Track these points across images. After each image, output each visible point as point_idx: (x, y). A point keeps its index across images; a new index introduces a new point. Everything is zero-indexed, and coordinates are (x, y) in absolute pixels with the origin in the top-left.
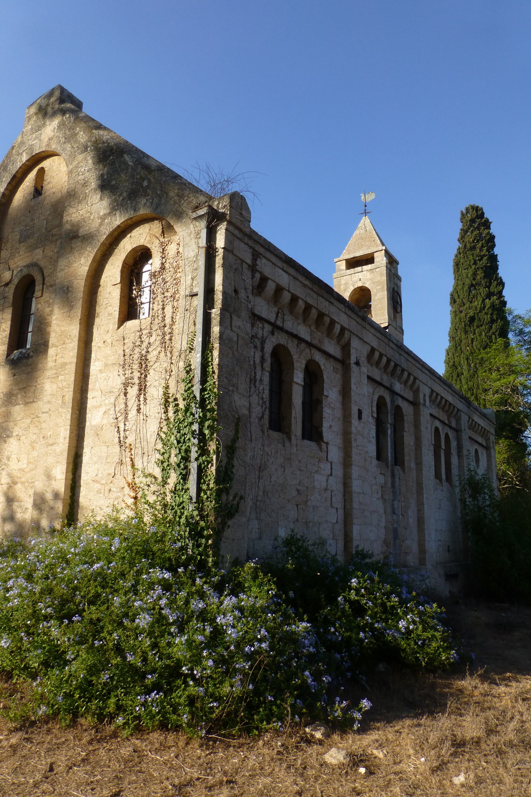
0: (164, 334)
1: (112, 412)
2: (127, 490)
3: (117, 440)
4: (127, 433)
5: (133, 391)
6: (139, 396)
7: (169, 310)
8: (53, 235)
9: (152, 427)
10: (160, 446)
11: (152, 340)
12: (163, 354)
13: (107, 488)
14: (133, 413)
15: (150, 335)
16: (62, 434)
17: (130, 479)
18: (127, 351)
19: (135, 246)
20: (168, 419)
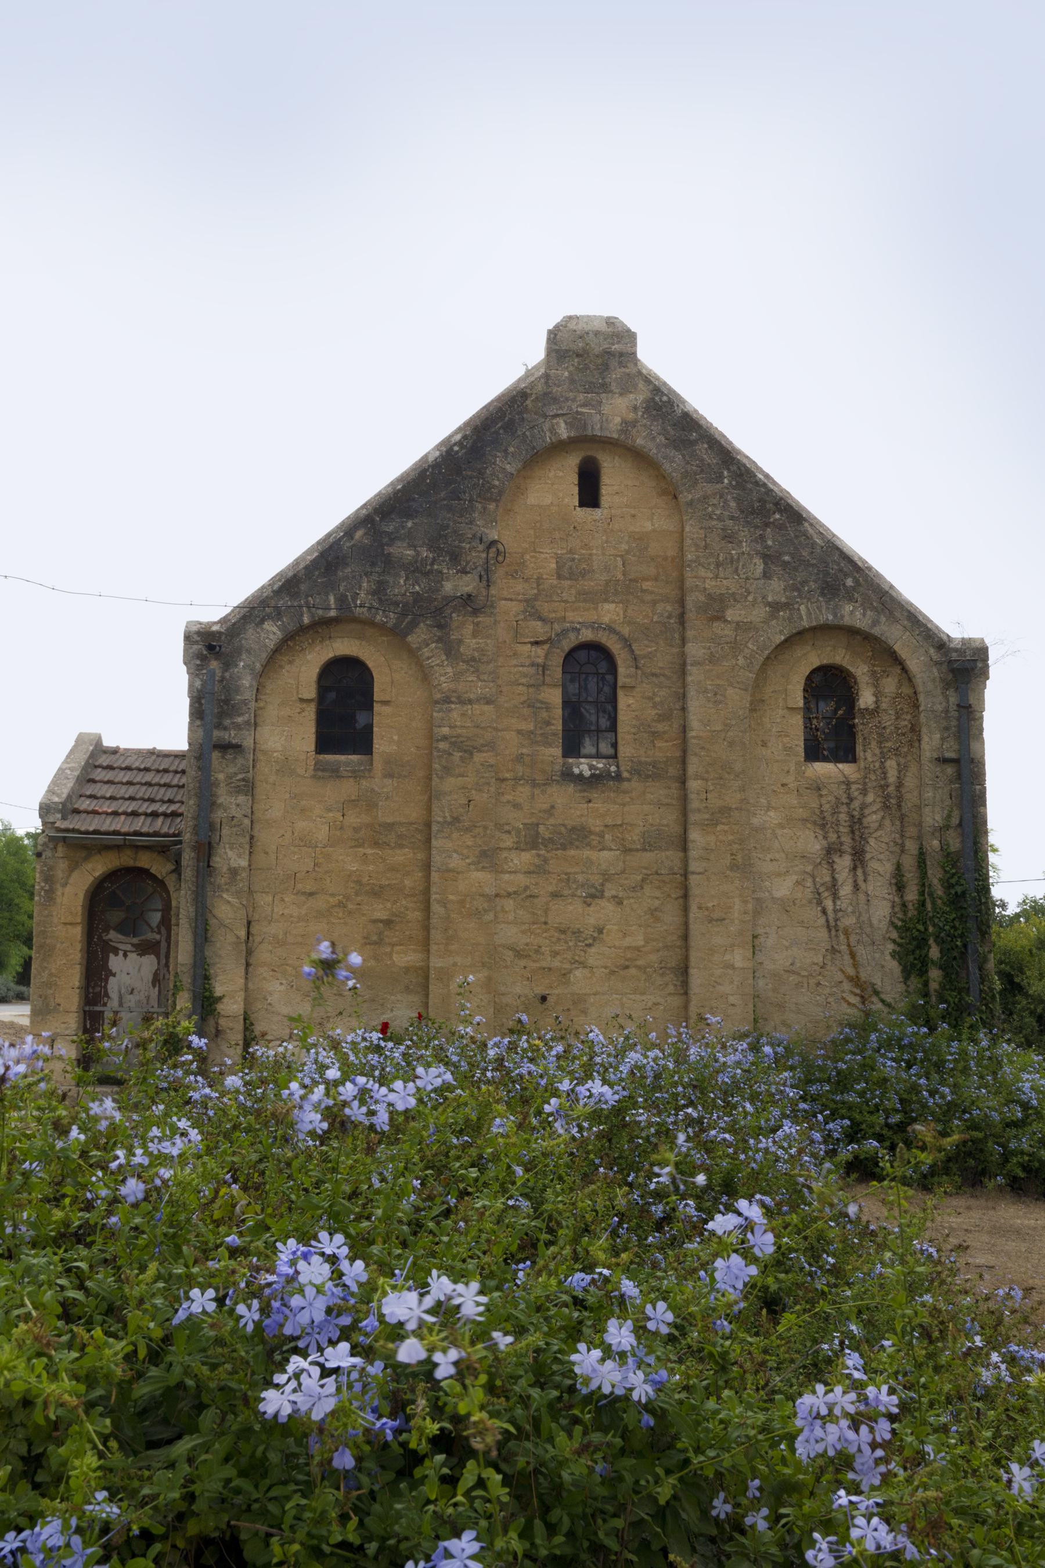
0: (887, 797)
1: (809, 883)
2: (847, 986)
3: (822, 921)
4: (840, 914)
5: (844, 863)
6: (855, 868)
7: (891, 764)
8: (643, 591)
9: (881, 910)
10: (895, 935)
11: (870, 798)
12: (887, 822)
13: (812, 981)
14: (846, 890)
15: (864, 792)
16: (736, 907)
17: (851, 971)
18: (826, 807)
19: (825, 662)
20: (904, 905)
